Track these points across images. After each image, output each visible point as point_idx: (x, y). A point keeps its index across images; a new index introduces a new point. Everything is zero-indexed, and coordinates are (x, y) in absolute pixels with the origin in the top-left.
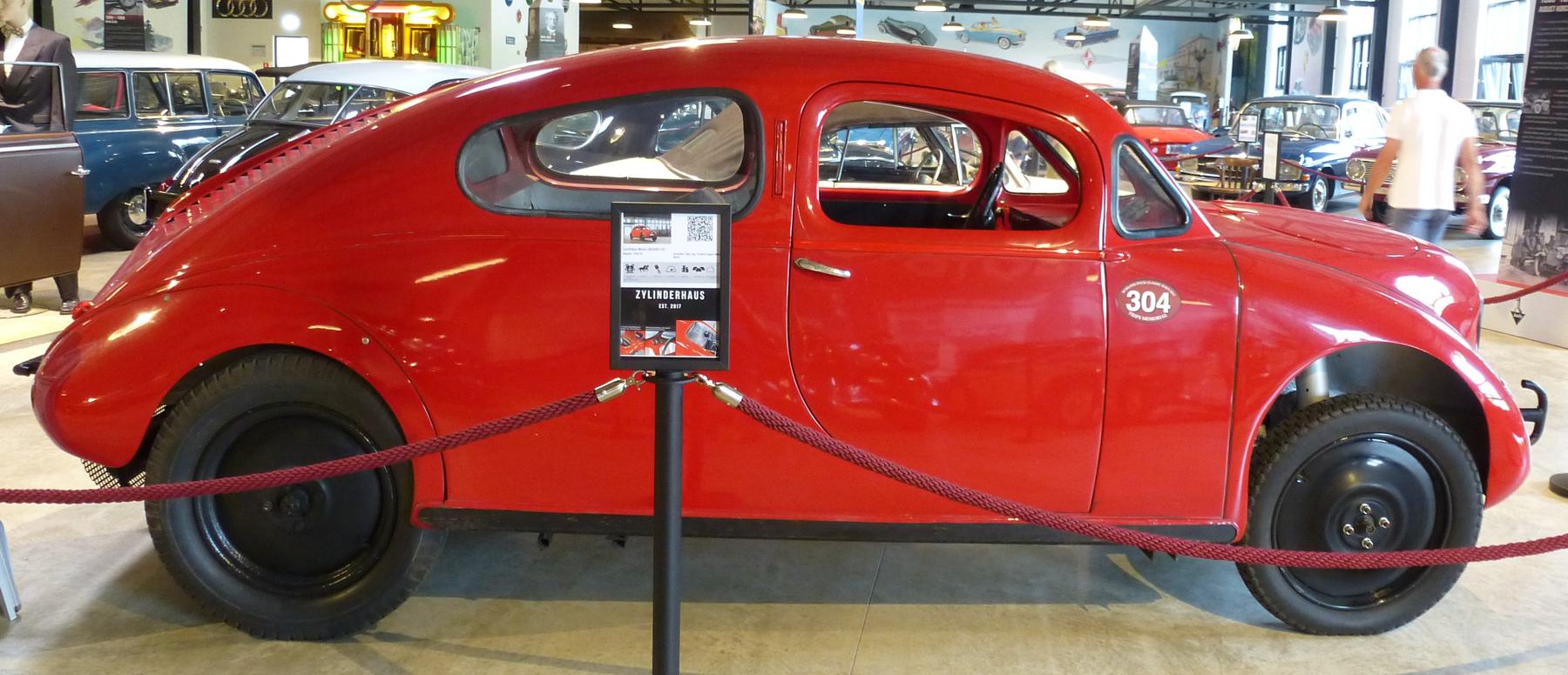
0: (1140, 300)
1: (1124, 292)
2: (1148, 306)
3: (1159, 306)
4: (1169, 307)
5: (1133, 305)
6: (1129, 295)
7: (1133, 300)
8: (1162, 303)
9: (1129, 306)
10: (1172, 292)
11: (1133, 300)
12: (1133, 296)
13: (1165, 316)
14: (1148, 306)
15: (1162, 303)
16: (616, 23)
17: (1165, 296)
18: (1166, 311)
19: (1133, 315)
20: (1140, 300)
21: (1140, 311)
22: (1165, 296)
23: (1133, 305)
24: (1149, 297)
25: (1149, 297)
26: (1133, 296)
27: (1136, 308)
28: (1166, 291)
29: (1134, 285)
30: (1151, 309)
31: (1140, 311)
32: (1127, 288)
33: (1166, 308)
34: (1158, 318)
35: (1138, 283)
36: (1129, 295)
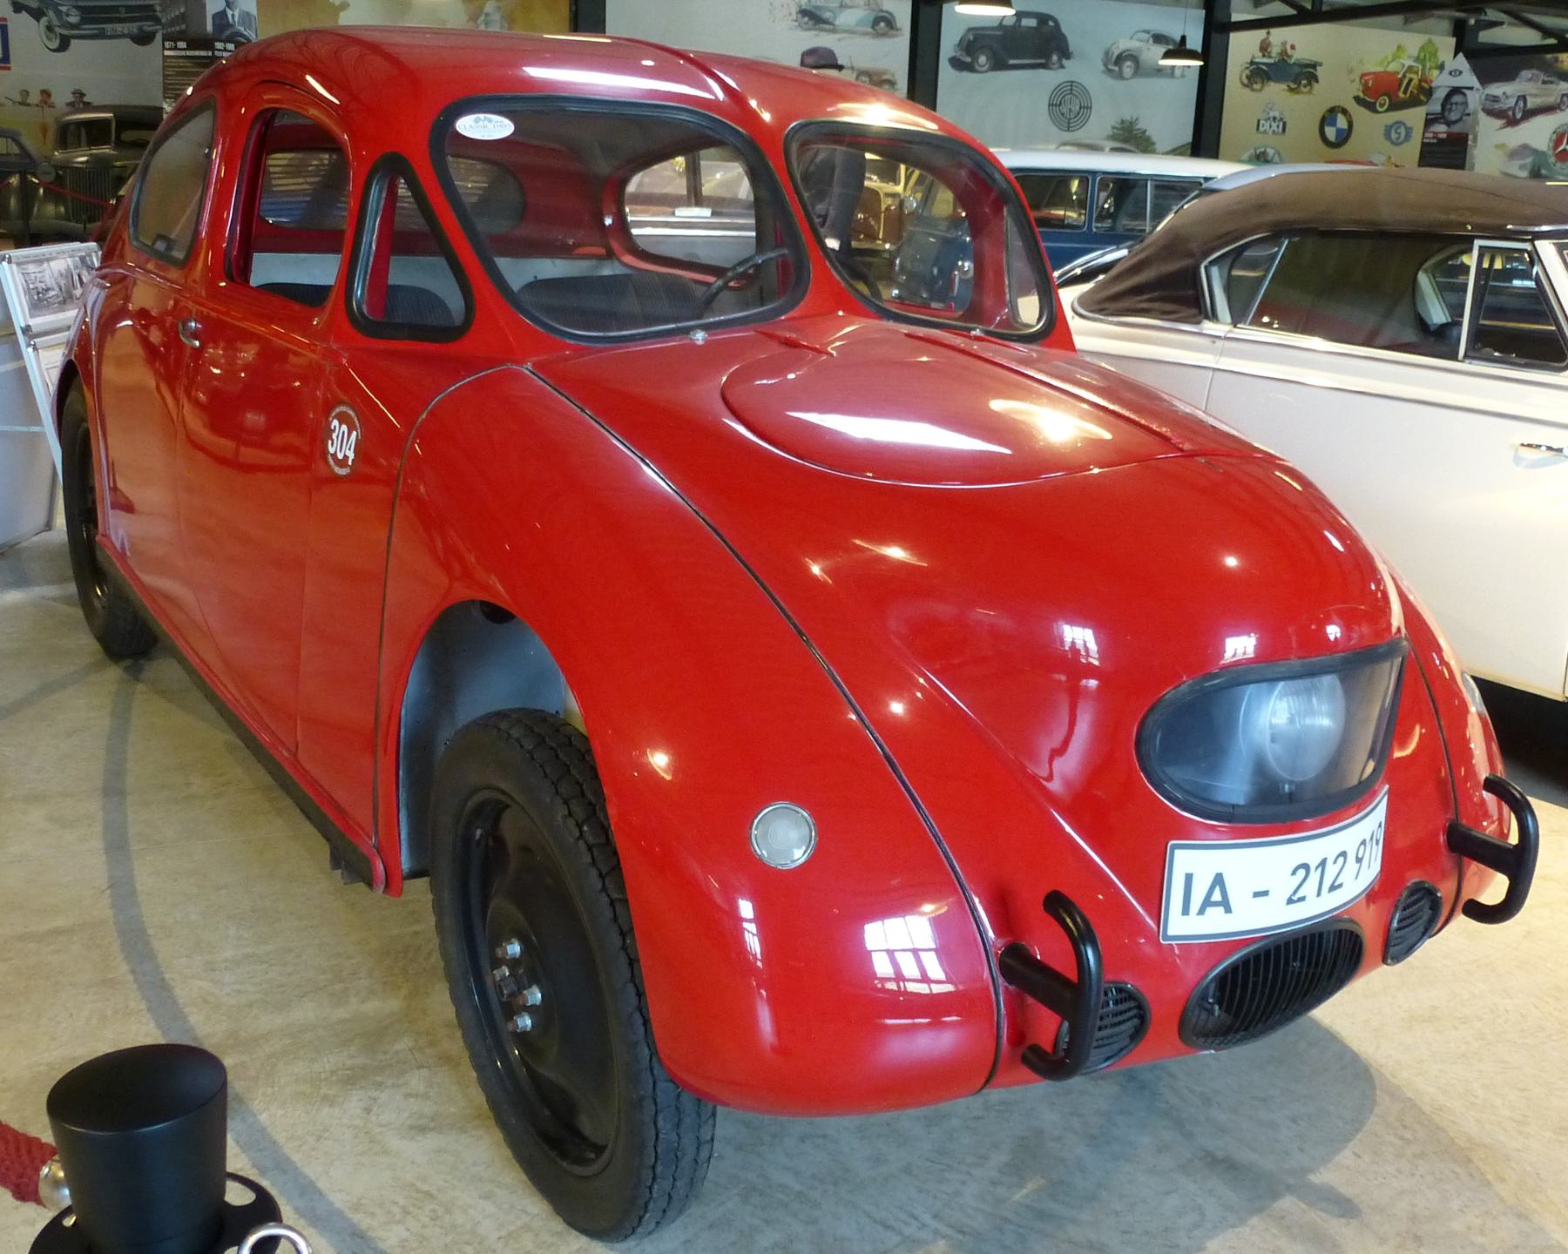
16: (311, 75)
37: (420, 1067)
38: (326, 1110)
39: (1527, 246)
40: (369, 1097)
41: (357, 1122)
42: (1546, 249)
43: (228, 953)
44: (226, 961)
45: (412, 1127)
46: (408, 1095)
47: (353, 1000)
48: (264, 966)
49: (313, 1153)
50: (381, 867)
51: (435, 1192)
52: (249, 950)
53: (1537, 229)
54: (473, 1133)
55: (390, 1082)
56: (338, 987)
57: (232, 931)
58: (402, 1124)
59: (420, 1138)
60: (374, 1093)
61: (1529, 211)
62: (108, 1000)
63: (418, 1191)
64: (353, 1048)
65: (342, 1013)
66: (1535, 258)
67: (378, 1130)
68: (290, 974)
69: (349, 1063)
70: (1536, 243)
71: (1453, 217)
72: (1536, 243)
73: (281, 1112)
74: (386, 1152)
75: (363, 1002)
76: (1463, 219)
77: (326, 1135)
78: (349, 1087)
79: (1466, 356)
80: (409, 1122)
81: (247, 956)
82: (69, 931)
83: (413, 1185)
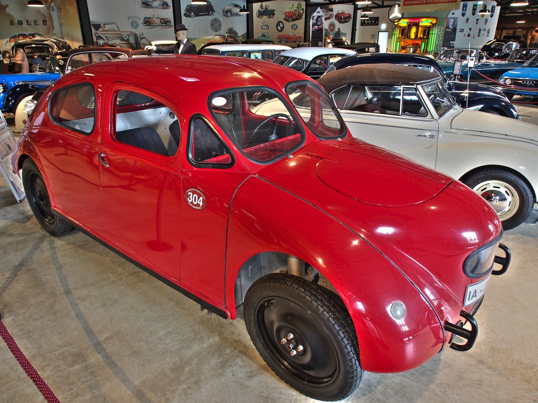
0: (192, 197)
1: (187, 192)
2: (195, 201)
3: (199, 202)
4: (202, 204)
5: (190, 199)
6: (189, 194)
7: (190, 197)
8: (200, 201)
9: (188, 199)
10: (204, 197)
11: (190, 197)
12: (190, 195)
13: (200, 208)
14: (195, 201)
15: (200, 201)
17: (201, 198)
18: (201, 206)
19: (190, 203)
20: (192, 197)
21: (192, 203)
22: (201, 198)
23: (190, 199)
24: (195, 197)
25: (195, 197)
26: (190, 195)
27: (191, 201)
28: (202, 197)
29: (190, 190)
30: (195, 203)
31: (192, 203)
32: (188, 191)
33: (201, 204)
34: (198, 208)
35: (192, 189)
36: (189, 194)
37: (237, 357)
38: (223, 378)
39: (415, 87)
40: (231, 370)
41: (234, 379)
42: (419, 87)
43: (161, 333)
44: (162, 336)
45: (248, 377)
46: (240, 367)
47: (206, 340)
48: (174, 335)
49: (229, 393)
50: (229, 313)
51: (268, 396)
52: (166, 331)
53: (416, 83)
54: (264, 374)
55: (233, 364)
56: (198, 337)
57: (157, 325)
58: (245, 376)
59: (252, 380)
60: (232, 369)
61: (415, 78)
62: (139, 359)
63: (263, 397)
64: (216, 356)
65: (205, 345)
66: (416, 89)
67: (240, 380)
68: (183, 336)
69: (219, 361)
70: (417, 86)
71: (396, 80)
72: (417, 86)
73: (212, 382)
74: (247, 387)
75: (208, 340)
76: (399, 81)
77: (228, 386)
78: (224, 369)
79: (401, 114)
80: (246, 375)
81: (167, 333)
82: (111, 338)
83: (261, 395)
